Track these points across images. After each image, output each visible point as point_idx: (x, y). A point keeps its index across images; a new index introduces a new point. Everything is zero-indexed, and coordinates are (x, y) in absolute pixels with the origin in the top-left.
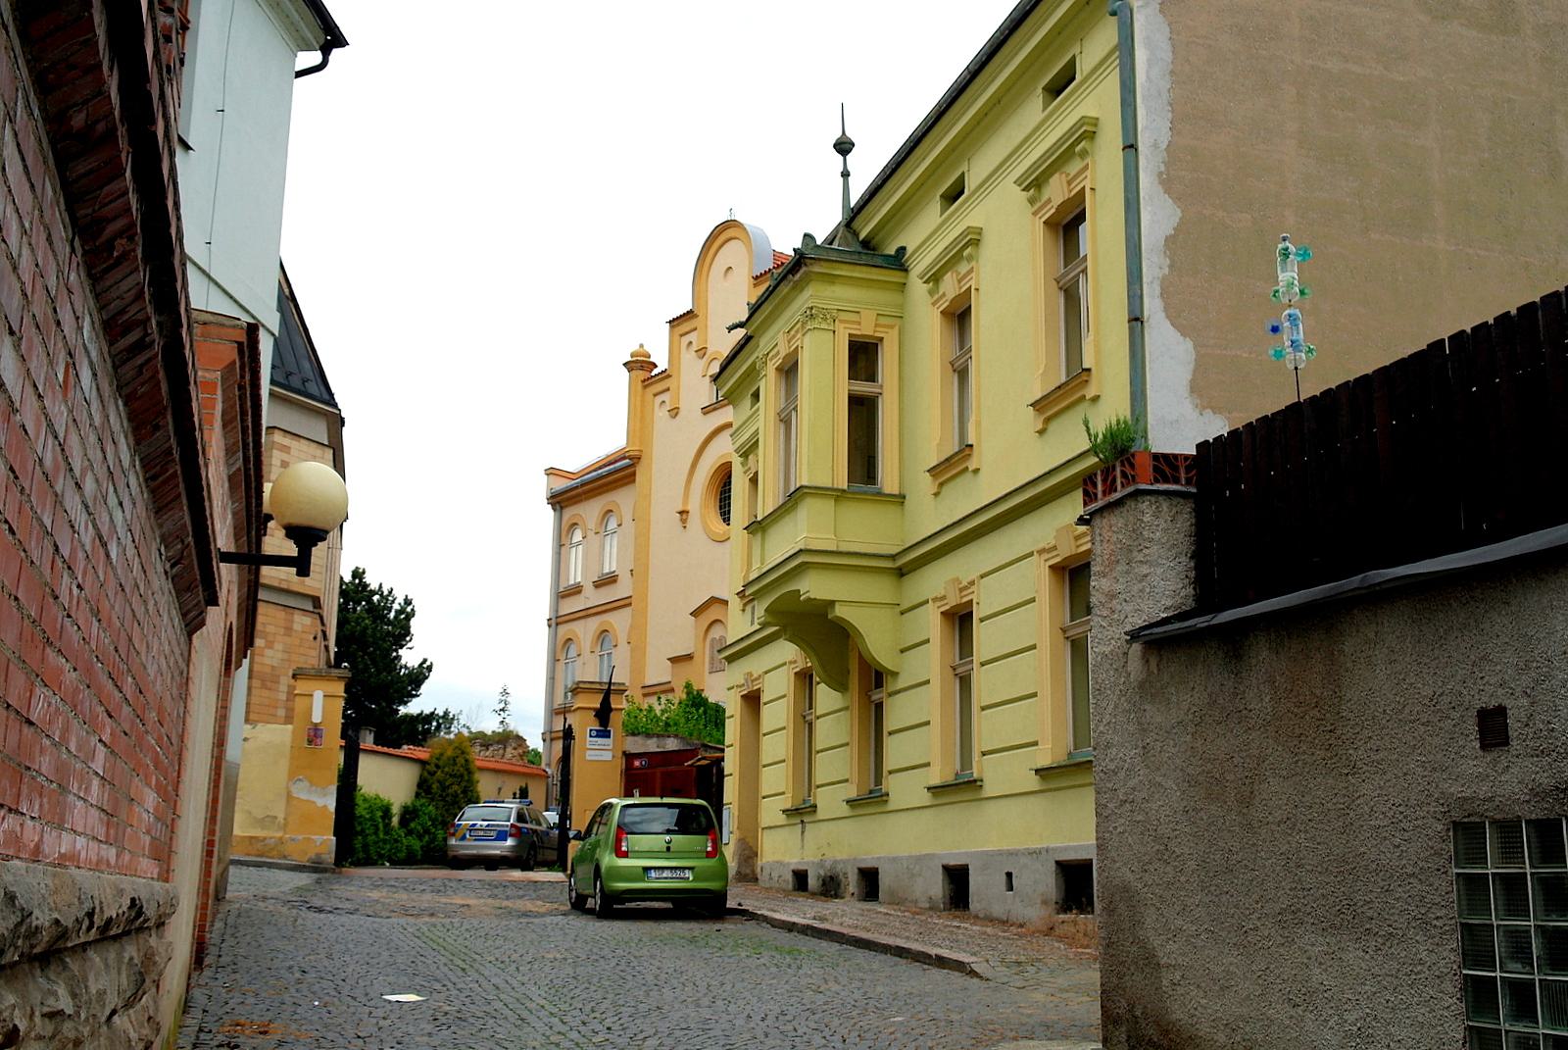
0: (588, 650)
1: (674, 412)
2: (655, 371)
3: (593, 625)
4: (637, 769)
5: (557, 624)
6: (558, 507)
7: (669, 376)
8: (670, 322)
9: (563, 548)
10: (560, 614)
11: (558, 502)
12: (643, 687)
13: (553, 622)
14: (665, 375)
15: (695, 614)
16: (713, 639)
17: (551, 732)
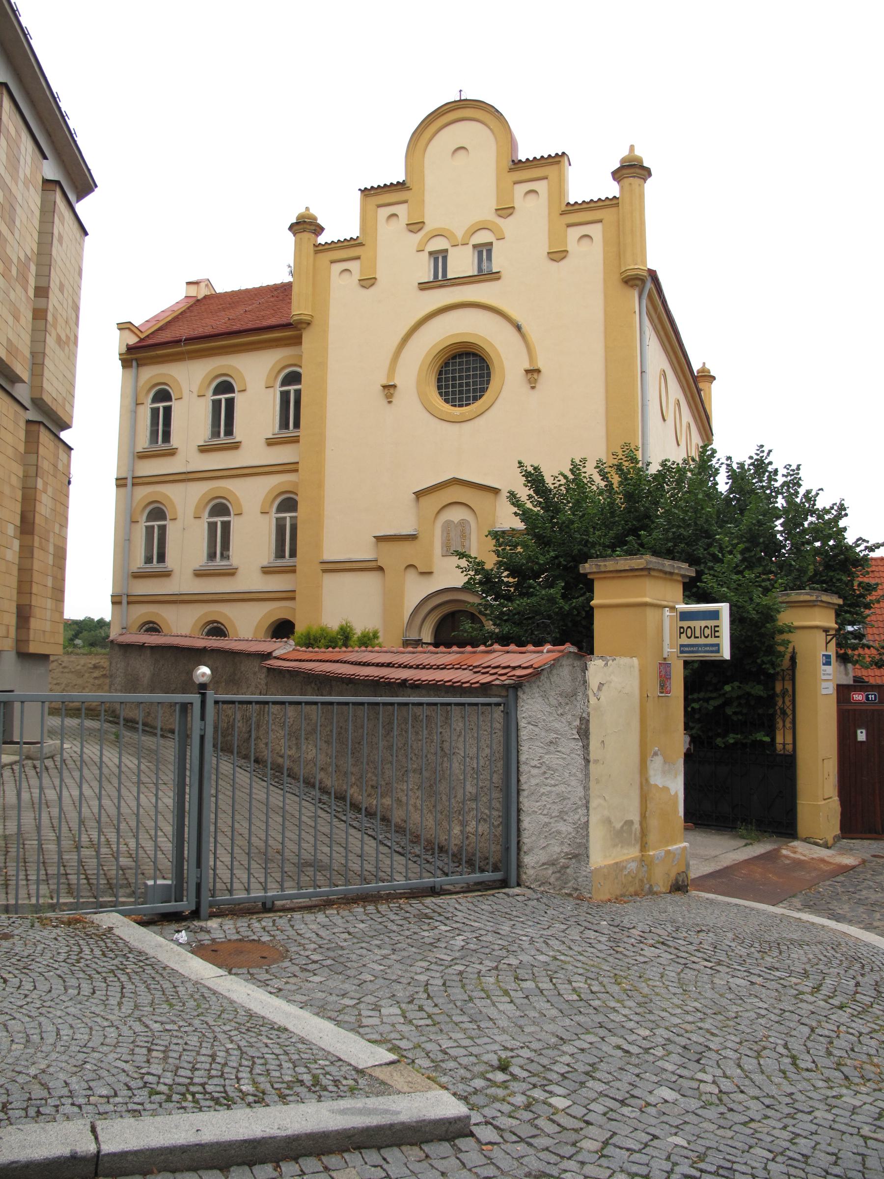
1: (368, 282)
2: (322, 239)
3: (198, 491)
4: (859, 703)
6: (134, 364)
7: (361, 244)
8: (366, 192)
9: (141, 409)
11: (136, 360)
13: (129, 482)
15: (419, 495)
16: (448, 524)
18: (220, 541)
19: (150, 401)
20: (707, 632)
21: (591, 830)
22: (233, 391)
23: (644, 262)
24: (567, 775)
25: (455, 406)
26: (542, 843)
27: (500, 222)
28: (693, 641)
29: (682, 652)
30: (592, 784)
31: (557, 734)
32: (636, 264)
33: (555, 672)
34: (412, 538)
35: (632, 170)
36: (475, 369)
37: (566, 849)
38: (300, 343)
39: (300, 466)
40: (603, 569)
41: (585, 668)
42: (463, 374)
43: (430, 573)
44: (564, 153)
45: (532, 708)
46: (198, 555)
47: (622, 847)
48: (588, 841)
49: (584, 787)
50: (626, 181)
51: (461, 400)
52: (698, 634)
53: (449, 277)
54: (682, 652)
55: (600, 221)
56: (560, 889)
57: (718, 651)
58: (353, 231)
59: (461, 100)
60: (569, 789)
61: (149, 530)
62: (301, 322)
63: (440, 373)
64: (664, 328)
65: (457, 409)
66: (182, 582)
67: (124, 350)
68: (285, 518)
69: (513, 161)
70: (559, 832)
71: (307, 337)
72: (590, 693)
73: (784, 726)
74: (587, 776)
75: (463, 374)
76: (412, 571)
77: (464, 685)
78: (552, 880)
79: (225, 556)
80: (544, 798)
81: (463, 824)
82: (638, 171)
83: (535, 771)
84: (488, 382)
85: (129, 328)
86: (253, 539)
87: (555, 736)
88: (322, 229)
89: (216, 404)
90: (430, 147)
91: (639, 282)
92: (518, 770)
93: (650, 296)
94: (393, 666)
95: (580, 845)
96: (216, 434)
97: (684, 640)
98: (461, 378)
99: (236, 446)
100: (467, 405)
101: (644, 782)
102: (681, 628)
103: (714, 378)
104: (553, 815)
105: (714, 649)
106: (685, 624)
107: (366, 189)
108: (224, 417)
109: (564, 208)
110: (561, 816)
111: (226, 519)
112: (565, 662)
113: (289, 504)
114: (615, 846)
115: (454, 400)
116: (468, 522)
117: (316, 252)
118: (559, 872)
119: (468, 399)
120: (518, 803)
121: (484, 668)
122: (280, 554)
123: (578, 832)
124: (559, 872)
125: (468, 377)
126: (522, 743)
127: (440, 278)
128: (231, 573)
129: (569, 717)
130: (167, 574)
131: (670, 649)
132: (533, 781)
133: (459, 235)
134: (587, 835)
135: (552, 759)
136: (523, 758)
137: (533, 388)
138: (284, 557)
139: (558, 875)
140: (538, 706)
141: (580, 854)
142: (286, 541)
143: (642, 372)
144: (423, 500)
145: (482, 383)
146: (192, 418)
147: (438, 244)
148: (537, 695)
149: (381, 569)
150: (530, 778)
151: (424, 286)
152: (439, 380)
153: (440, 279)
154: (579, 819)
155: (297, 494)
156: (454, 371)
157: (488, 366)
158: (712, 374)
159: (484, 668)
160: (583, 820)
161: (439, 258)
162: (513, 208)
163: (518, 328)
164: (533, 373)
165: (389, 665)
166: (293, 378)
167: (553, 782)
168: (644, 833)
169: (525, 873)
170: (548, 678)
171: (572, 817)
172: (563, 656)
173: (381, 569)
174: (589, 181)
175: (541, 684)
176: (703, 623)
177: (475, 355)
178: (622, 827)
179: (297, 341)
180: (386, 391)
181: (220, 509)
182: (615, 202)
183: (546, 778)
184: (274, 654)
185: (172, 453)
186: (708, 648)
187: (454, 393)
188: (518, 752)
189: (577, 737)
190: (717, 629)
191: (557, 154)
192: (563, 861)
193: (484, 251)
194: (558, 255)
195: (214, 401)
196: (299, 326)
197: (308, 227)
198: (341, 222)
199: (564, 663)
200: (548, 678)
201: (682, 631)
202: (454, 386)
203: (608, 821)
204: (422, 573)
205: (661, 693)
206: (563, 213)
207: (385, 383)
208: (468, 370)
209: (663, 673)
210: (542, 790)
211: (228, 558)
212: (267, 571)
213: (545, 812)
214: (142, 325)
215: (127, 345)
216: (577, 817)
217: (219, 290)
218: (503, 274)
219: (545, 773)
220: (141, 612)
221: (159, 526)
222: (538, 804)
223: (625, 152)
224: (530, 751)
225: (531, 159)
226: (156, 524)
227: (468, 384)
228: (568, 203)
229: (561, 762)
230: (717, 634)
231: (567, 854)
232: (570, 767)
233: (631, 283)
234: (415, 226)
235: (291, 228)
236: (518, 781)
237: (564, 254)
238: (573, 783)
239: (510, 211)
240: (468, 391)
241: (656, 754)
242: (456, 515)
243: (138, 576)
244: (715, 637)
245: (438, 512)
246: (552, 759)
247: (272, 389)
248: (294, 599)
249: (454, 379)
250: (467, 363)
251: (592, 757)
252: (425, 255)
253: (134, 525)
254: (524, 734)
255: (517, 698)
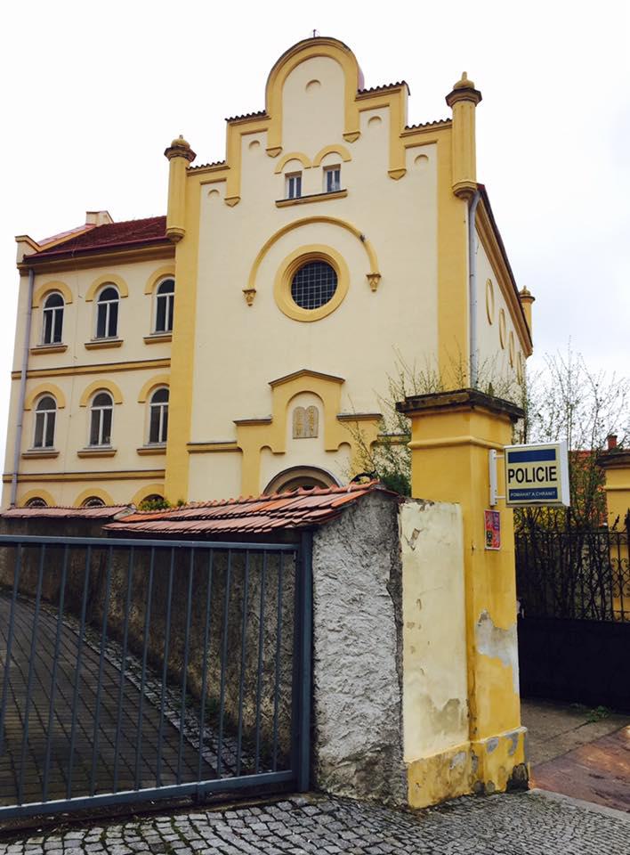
0: (77, 403)
1: (233, 201)
2: (193, 164)
3: (86, 384)
5: (27, 377)
6: (30, 272)
7: (227, 168)
8: (232, 122)
9: (35, 311)
10: (29, 369)
11: (32, 269)
12: (188, 445)
14: (220, 167)
15: (274, 384)
16: (298, 412)
17: (18, 475)
18: (102, 426)
19: (44, 305)
20: (542, 474)
21: (404, 712)
22: (117, 297)
23: (474, 175)
24: (373, 641)
25: (306, 308)
26: (343, 731)
27: (347, 145)
28: (525, 485)
29: (511, 498)
30: (406, 653)
31: (362, 590)
32: (467, 178)
33: (359, 513)
34: (267, 422)
35: (465, 94)
36: (324, 276)
37: (374, 739)
38: (174, 256)
39: (172, 362)
40: (421, 406)
41: (396, 511)
42: (313, 281)
43: (283, 453)
44: (403, 82)
45: (330, 555)
46: (82, 439)
47: (445, 734)
48: (401, 728)
49: (397, 657)
50: (458, 105)
51: (312, 303)
52: (530, 477)
53: (303, 195)
54: (511, 498)
55: (435, 142)
56: (367, 794)
57: (555, 496)
58: (219, 155)
59: (315, 38)
60: (377, 659)
61: (40, 417)
62: (174, 235)
63: (294, 281)
64: (490, 241)
65: (308, 310)
66: (68, 462)
67: (21, 260)
68: (159, 407)
69: (359, 91)
70: (364, 716)
71: (180, 249)
72: (403, 541)
73: (621, 592)
74: (399, 642)
75: (313, 281)
76: (266, 452)
77: (256, 531)
78: (355, 781)
79: (106, 441)
80: (345, 671)
81: (257, 700)
82: (471, 94)
83: (333, 636)
84: (335, 288)
85: (26, 241)
86: (130, 425)
87: (360, 592)
88: (194, 155)
89: (102, 309)
90: (286, 83)
91: (469, 195)
92: (313, 635)
93: (478, 209)
94: (201, 519)
95: (390, 734)
96: (101, 332)
97: (514, 485)
98: (312, 284)
99: (118, 344)
100: (316, 307)
101: (471, 650)
102: (510, 470)
103: (534, 299)
104: (357, 693)
105: (550, 494)
106: (515, 466)
107: (231, 118)
108: (108, 321)
109: (403, 131)
110: (367, 695)
111: (108, 407)
112: (371, 502)
113: (162, 395)
114: (437, 732)
115: (305, 303)
116: (317, 409)
117: (189, 175)
118: (364, 770)
119: (318, 302)
120: (313, 677)
121: (282, 512)
122: (154, 438)
123: (388, 716)
124: (364, 770)
125: (318, 283)
126: (317, 601)
127: (295, 196)
128: (111, 454)
129: (377, 568)
130: (54, 456)
131: (499, 495)
132: (332, 649)
133: (312, 156)
134: (401, 720)
135: (355, 621)
136: (318, 619)
137: (374, 291)
138: (157, 441)
139: (363, 774)
140: (338, 554)
141: (391, 747)
142: (158, 428)
143: (471, 276)
144: (277, 390)
145: (330, 288)
146: (80, 322)
147: (293, 168)
148: (336, 541)
149: (239, 450)
150: (327, 646)
151: (281, 204)
152: (293, 286)
153: (295, 197)
154: (390, 699)
155: (168, 386)
156: (306, 279)
157: (335, 273)
158: (532, 295)
159: (282, 512)
160: (396, 699)
161: (294, 179)
162: (359, 133)
163: (362, 239)
164: (374, 277)
165: (198, 518)
166: (168, 286)
167: (356, 650)
168: (472, 716)
169: (321, 772)
170: (351, 520)
171: (381, 696)
172: (368, 494)
173: (239, 450)
174: (426, 106)
175: (341, 528)
176: (536, 465)
177: (325, 264)
178: (445, 708)
179: (171, 254)
180: (247, 296)
181: (103, 398)
182: (448, 124)
183: (348, 645)
184: (115, 517)
185: (62, 350)
186: (543, 493)
187: (306, 297)
188: (313, 611)
189: (387, 593)
190: (553, 470)
191: (398, 83)
192: (370, 754)
193: (333, 173)
194: (398, 174)
195: (100, 306)
196: (173, 239)
197: (180, 151)
198: (209, 149)
199: (370, 503)
200: (351, 520)
201: (511, 474)
202: (306, 291)
203: (428, 700)
204: (276, 454)
205: (489, 545)
206: (403, 136)
207: (247, 288)
208: (318, 277)
209: (490, 523)
210: (343, 661)
211: (109, 442)
212: (142, 453)
213: (346, 690)
214: (40, 242)
215: (24, 256)
216: (387, 696)
217: (116, 220)
218: (349, 192)
219: (346, 638)
220: (29, 490)
221: (49, 414)
222: (338, 678)
223: (458, 79)
224: (327, 612)
225: (375, 88)
226: (46, 412)
227: (318, 290)
228: (407, 127)
229: (366, 624)
230: (553, 476)
231: (374, 745)
232: (379, 631)
233: (461, 196)
234: (274, 151)
235: (165, 154)
236: (313, 648)
237: (403, 172)
238: (382, 652)
239: (355, 136)
240: (318, 296)
241: (484, 618)
242: (306, 402)
243: (27, 457)
244: (551, 480)
245: (291, 400)
246: (355, 621)
247: (150, 296)
248: (163, 477)
249: (306, 285)
250: (318, 271)
251: (405, 619)
252: (283, 176)
253: (26, 413)
254: (320, 589)
255: (312, 544)
